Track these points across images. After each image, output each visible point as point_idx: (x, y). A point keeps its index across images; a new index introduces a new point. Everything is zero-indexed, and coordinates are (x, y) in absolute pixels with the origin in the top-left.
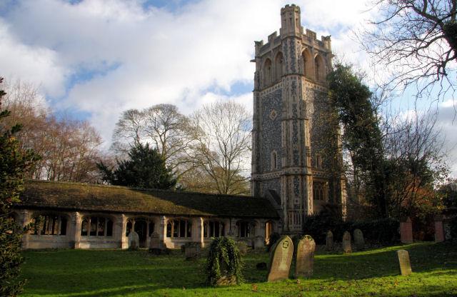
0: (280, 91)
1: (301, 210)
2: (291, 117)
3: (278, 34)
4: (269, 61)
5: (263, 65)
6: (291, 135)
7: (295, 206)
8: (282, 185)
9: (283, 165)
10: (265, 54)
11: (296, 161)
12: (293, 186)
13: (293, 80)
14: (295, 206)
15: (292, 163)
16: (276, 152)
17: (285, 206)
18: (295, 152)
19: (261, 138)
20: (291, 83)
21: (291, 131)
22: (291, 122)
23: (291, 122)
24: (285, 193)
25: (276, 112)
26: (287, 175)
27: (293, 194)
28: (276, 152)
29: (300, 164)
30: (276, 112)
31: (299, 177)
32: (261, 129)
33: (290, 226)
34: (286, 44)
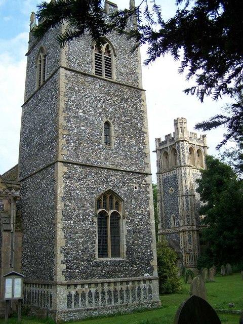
0: (176, 175)
1: (193, 253)
2: (184, 194)
3: (172, 136)
4: (166, 154)
5: (162, 155)
6: (185, 206)
7: (189, 250)
8: (180, 237)
9: (181, 224)
10: (163, 149)
11: (188, 222)
12: (187, 237)
13: (185, 169)
14: (189, 250)
15: (186, 223)
16: (175, 216)
17: (183, 250)
18: (188, 216)
19: (163, 205)
20: (183, 172)
21: (185, 203)
22: (184, 197)
23: (184, 197)
24: (183, 242)
25: (173, 189)
26: (184, 231)
27: (188, 243)
28: (175, 216)
29: (191, 224)
30: (173, 189)
31: (191, 232)
32: (163, 199)
33: (187, 263)
34: (179, 145)
